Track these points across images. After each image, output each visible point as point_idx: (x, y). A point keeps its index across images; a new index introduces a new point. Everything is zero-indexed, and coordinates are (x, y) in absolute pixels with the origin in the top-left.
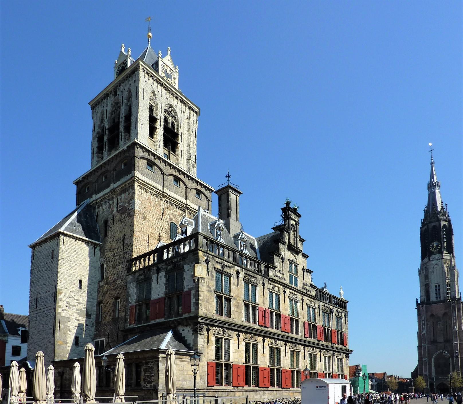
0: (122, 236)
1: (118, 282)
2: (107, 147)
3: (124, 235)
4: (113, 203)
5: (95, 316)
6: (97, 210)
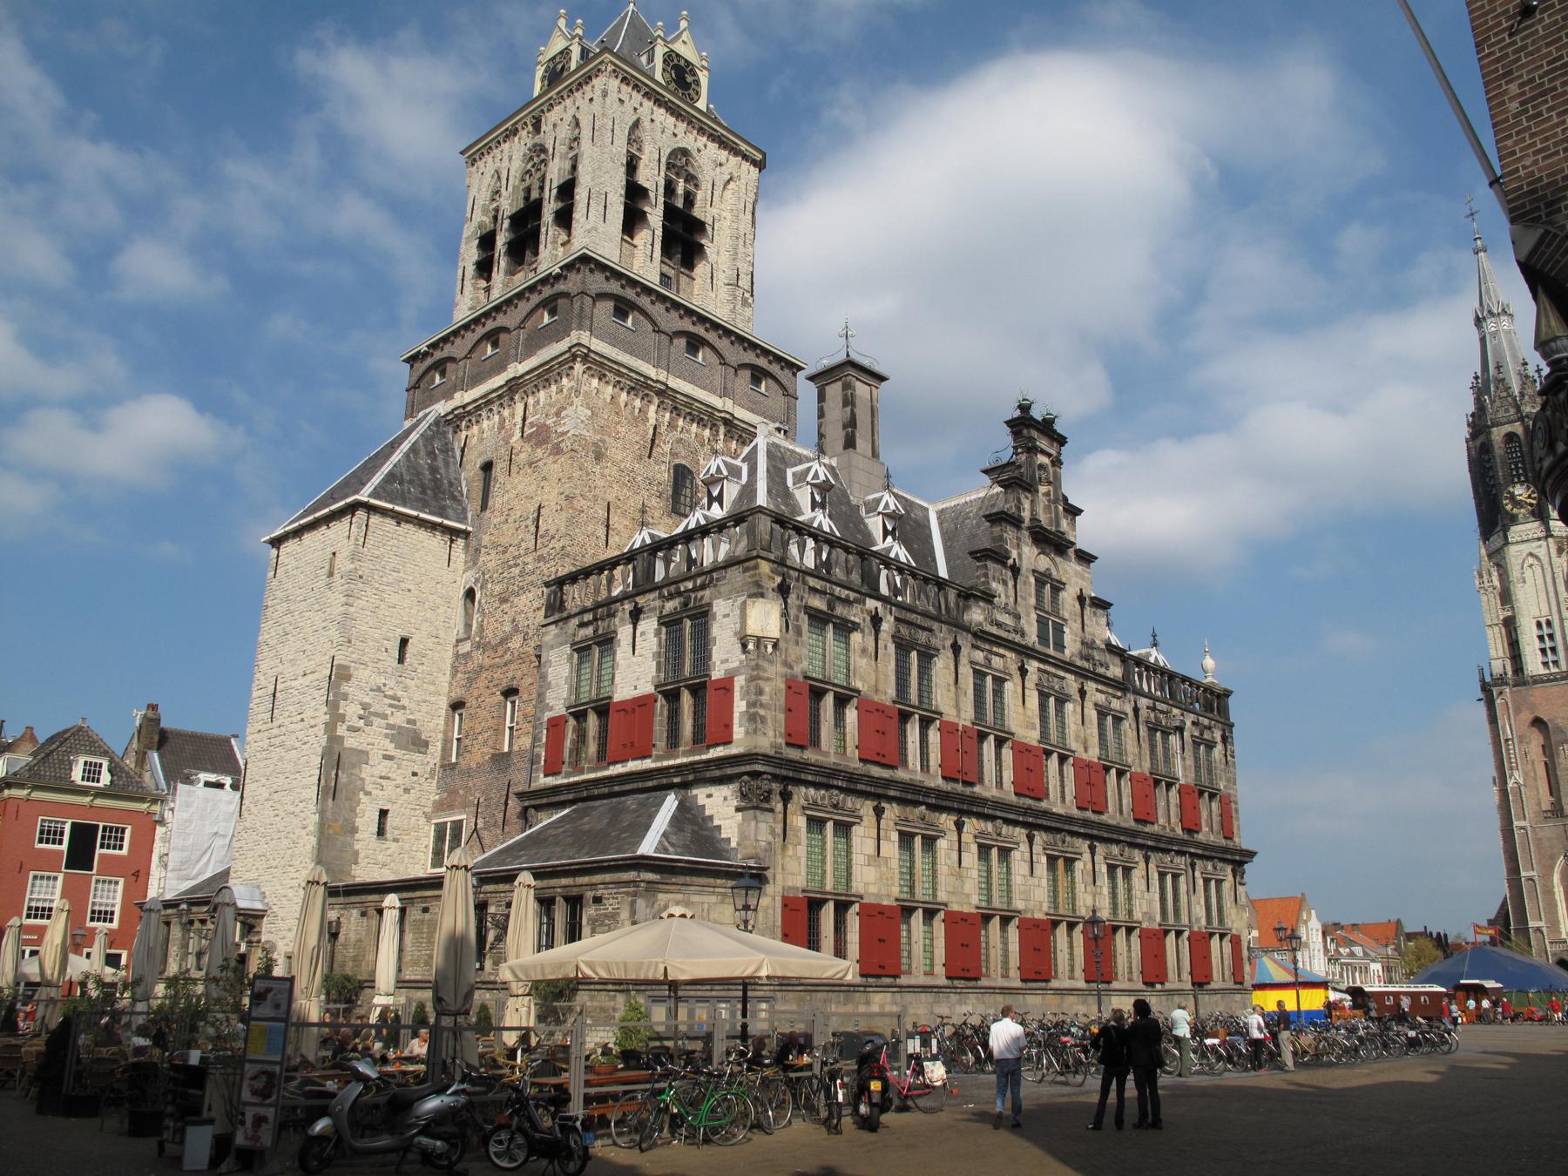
0: (533, 508)
1: (516, 643)
2: (503, 264)
4: (513, 415)
5: (439, 745)
6: (464, 434)
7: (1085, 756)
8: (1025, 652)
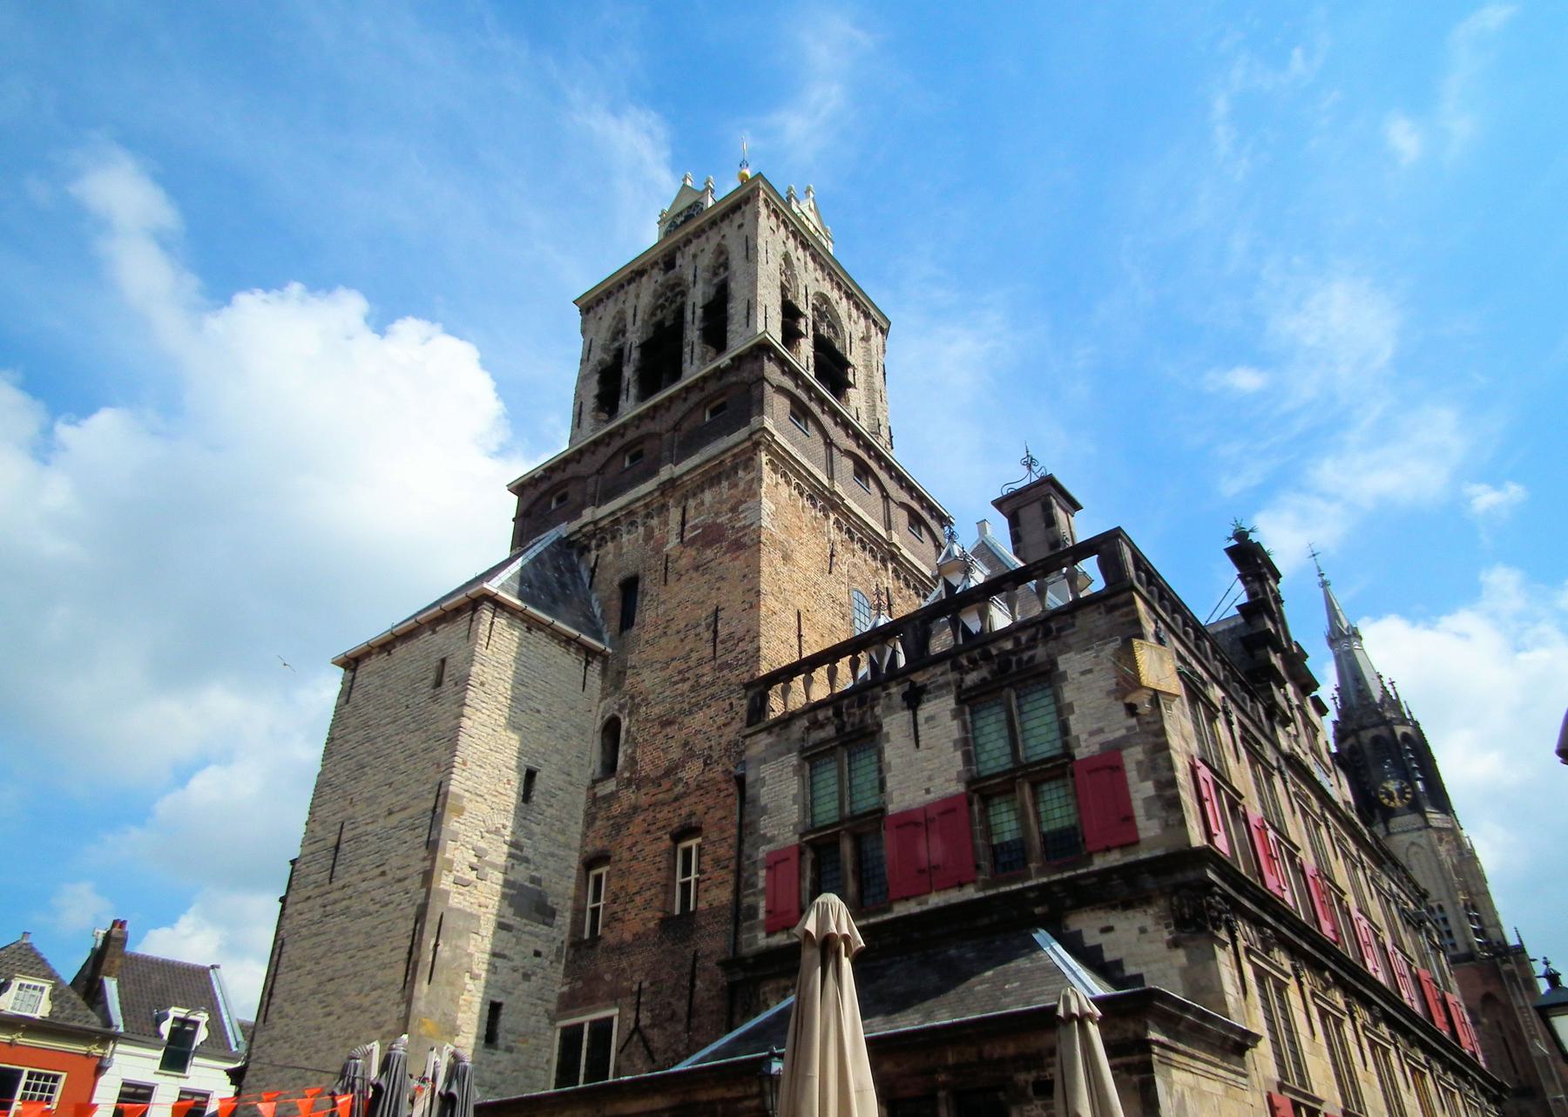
0: (704, 613)
3: (717, 610)
4: (666, 523)
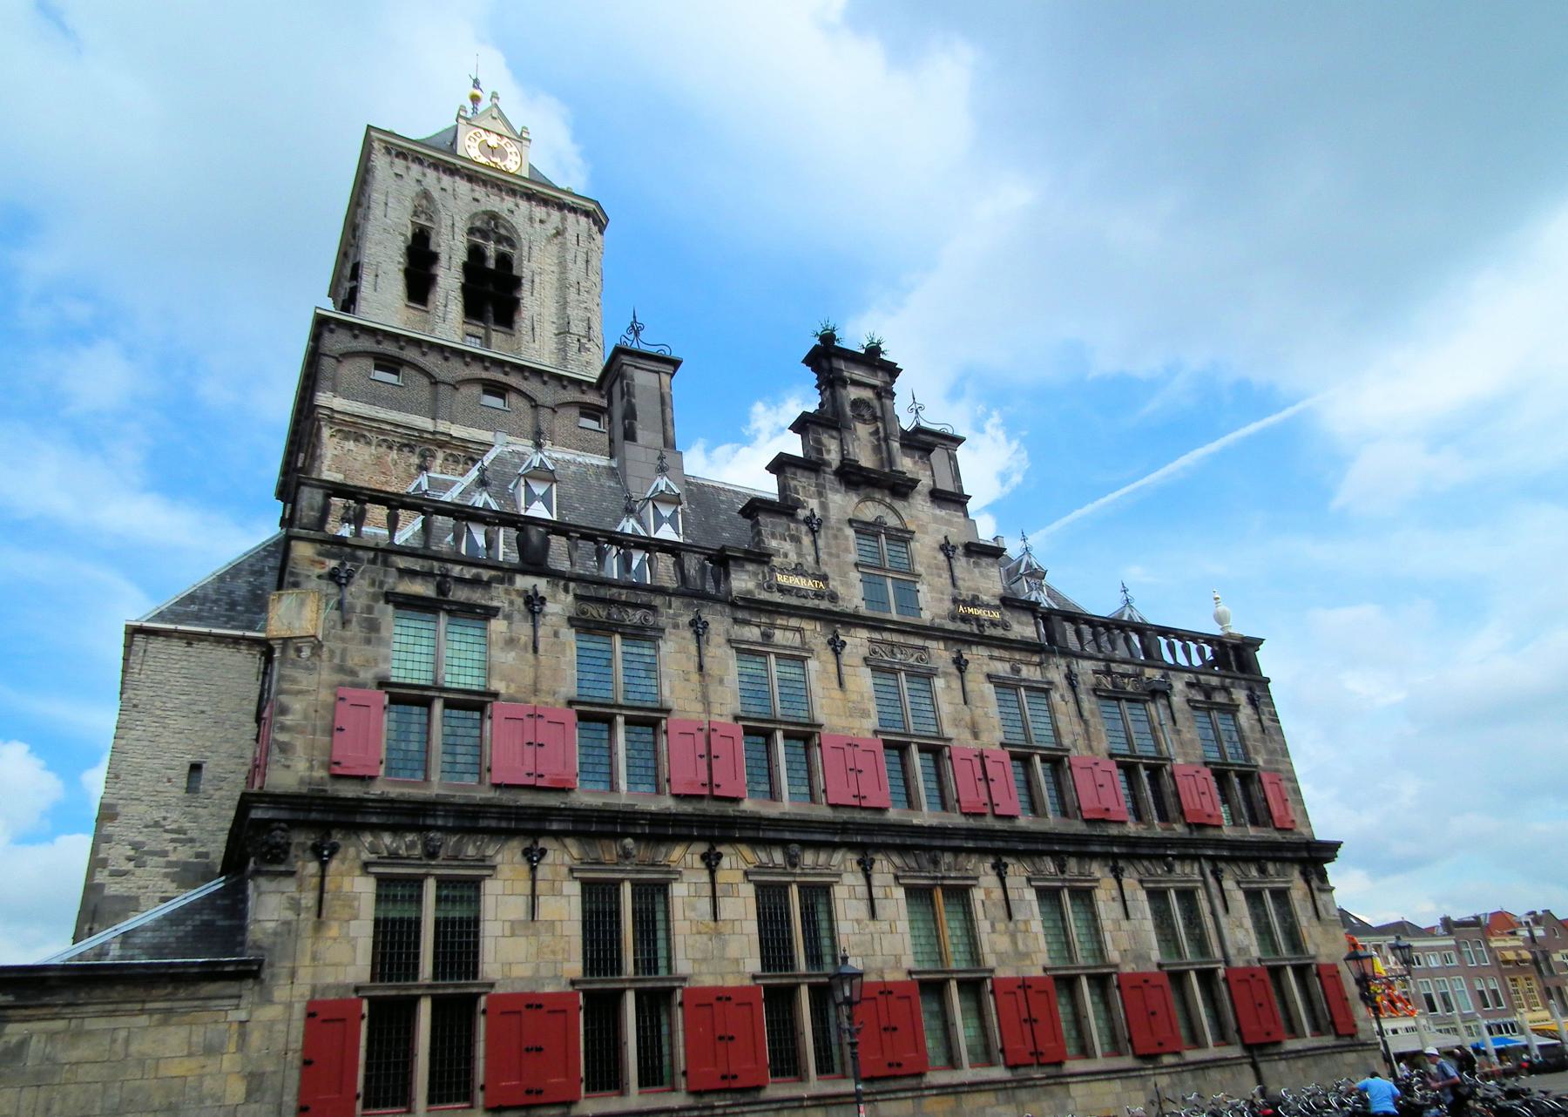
7: (973, 745)
8: (837, 620)
